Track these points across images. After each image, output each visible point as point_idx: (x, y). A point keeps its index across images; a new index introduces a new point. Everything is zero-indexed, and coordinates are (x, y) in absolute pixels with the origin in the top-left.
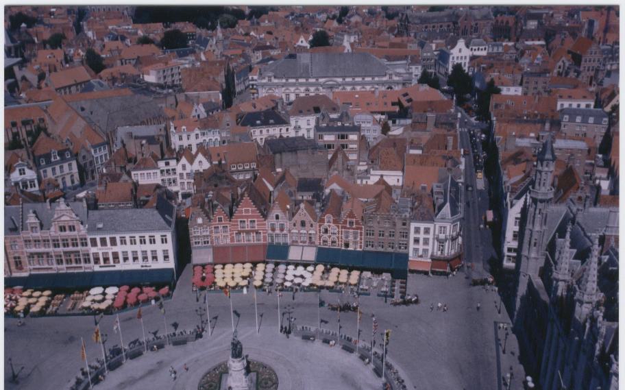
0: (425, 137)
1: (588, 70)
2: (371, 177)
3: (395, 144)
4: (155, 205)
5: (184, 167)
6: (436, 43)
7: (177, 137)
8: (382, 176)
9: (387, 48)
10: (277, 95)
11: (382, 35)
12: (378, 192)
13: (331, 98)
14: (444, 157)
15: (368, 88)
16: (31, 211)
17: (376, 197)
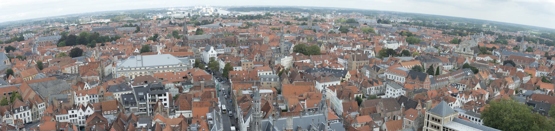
0: (200, 93)
1: (268, 58)
2: (176, 114)
5: (81, 114)
6: (201, 49)
7: (77, 98)
10: (126, 76)
11: (175, 46)
12: (181, 121)
13: (153, 76)
15: (171, 71)
17: (179, 124)
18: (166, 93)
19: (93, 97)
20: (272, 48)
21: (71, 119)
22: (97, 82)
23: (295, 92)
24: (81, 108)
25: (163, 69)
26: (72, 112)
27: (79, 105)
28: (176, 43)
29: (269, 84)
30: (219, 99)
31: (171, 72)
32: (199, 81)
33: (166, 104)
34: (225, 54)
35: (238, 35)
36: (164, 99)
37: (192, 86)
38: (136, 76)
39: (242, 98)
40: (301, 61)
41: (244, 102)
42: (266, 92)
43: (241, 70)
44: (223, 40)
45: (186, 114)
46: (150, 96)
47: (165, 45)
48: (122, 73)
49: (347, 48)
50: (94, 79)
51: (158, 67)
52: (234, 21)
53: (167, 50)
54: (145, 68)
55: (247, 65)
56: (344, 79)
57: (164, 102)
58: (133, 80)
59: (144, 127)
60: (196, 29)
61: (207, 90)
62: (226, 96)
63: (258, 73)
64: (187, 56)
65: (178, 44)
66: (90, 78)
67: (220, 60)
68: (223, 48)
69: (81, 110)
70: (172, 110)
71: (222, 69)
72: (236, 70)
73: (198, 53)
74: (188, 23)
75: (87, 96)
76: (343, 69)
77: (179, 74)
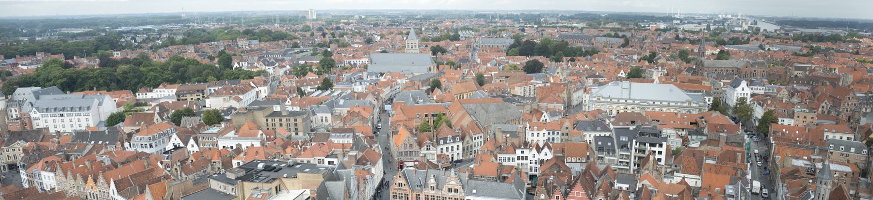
0: (717, 150)
1: (847, 111)
2: (674, 177)
4: (513, 181)
5: (534, 157)
7: (530, 133)
8: (684, 178)
10: (603, 110)
11: (682, 73)
13: (644, 115)
14: (734, 168)
15: (672, 110)
16: (432, 176)
18: (663, 142)
19: (554, 133)
20: (858, 95)
21: (519, 161)
22: (560, 113)
24: (534, 148)
25: (661, 106)
26: (522, 151)
27: (532, 143)
28: (683, 68)
29: (845, 155)
31: (672, 112)
32: (717, 132)
33: (660, 160)
34: (766, 95)
35: (791, 66)
36: (659, 152)
37: (704, 138)
38: (618, 112)
39: (791, 171)
41: (794, 179)
42: (838, 169)
43: (792, 125)
44: (764, 71)
46: (638, 143)
47: (665, 70)
48: (598, 105)
50: (556, 108)
51: (654, 103)
52: (786, 42)
53: (668, 78)
54: (634, 101)
55: (805, 117)
57: (657, 156)
58: (614, 117)
59: (624, 189)
60: (718, 50)
61: (730, 148)
62: (760, 162)
63: (825, 134)
64: (700, 91)
65: (686, 71)
66: (551, 106)
67: (756, 103)
68: (764, 85)
69: (534, 151)
70: (669, 170)
72: (782, 123)
73: (718, 89)
74: (707, 40)
75: (544, 131)
77: (685, 117)
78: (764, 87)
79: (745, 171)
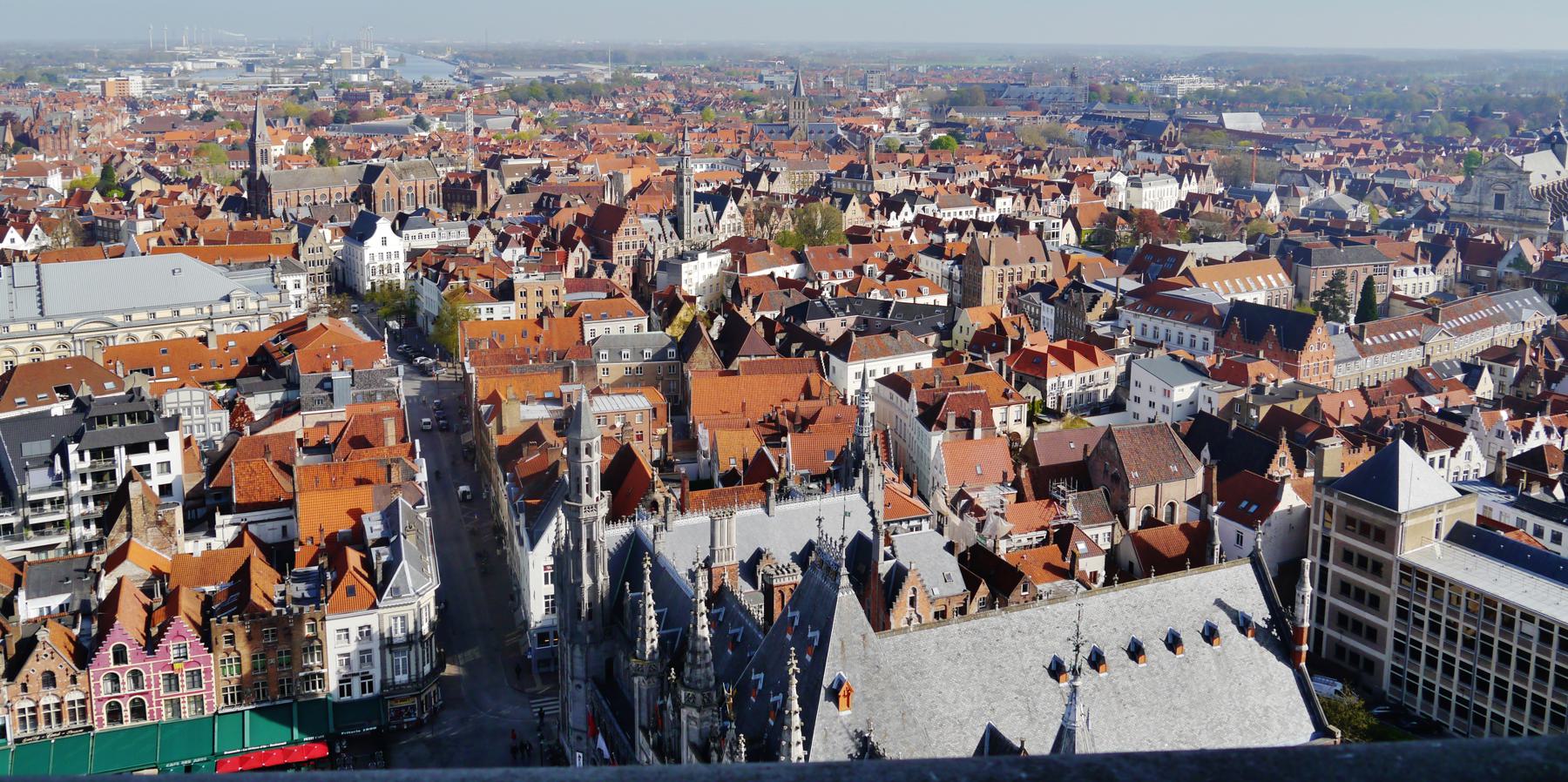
2: (218, 531)
3: (266, 447)
9: (224, 242)
11: (210, 217)
13: (100, 361)
18: (168, 434)
23: (744, 405)
25: (154, 322)
30: (418, 449)
40: (767, 272)
43: (513, 317)
45: (270, 525)
46: (87, 455)
49: (958, 210)
55: (540, 293)
56: (946, 344)
71: (427, 315)
76: (942, 300)
77: (231, 343)
78: (436, 230)
79: (410, 463)
